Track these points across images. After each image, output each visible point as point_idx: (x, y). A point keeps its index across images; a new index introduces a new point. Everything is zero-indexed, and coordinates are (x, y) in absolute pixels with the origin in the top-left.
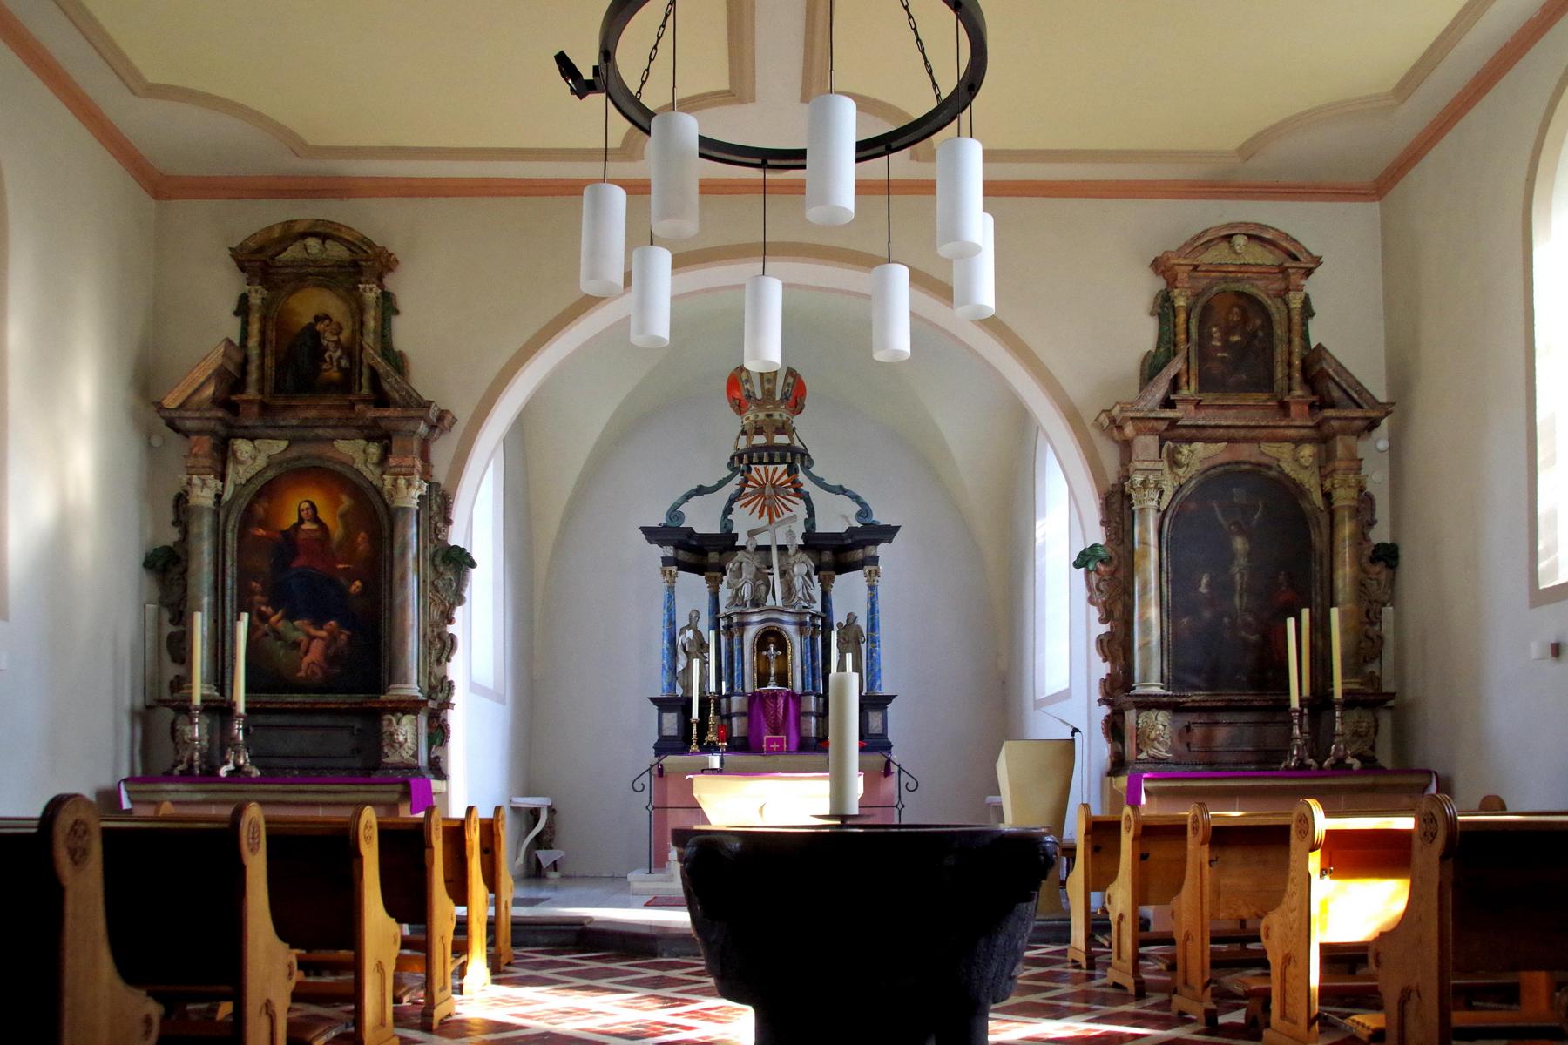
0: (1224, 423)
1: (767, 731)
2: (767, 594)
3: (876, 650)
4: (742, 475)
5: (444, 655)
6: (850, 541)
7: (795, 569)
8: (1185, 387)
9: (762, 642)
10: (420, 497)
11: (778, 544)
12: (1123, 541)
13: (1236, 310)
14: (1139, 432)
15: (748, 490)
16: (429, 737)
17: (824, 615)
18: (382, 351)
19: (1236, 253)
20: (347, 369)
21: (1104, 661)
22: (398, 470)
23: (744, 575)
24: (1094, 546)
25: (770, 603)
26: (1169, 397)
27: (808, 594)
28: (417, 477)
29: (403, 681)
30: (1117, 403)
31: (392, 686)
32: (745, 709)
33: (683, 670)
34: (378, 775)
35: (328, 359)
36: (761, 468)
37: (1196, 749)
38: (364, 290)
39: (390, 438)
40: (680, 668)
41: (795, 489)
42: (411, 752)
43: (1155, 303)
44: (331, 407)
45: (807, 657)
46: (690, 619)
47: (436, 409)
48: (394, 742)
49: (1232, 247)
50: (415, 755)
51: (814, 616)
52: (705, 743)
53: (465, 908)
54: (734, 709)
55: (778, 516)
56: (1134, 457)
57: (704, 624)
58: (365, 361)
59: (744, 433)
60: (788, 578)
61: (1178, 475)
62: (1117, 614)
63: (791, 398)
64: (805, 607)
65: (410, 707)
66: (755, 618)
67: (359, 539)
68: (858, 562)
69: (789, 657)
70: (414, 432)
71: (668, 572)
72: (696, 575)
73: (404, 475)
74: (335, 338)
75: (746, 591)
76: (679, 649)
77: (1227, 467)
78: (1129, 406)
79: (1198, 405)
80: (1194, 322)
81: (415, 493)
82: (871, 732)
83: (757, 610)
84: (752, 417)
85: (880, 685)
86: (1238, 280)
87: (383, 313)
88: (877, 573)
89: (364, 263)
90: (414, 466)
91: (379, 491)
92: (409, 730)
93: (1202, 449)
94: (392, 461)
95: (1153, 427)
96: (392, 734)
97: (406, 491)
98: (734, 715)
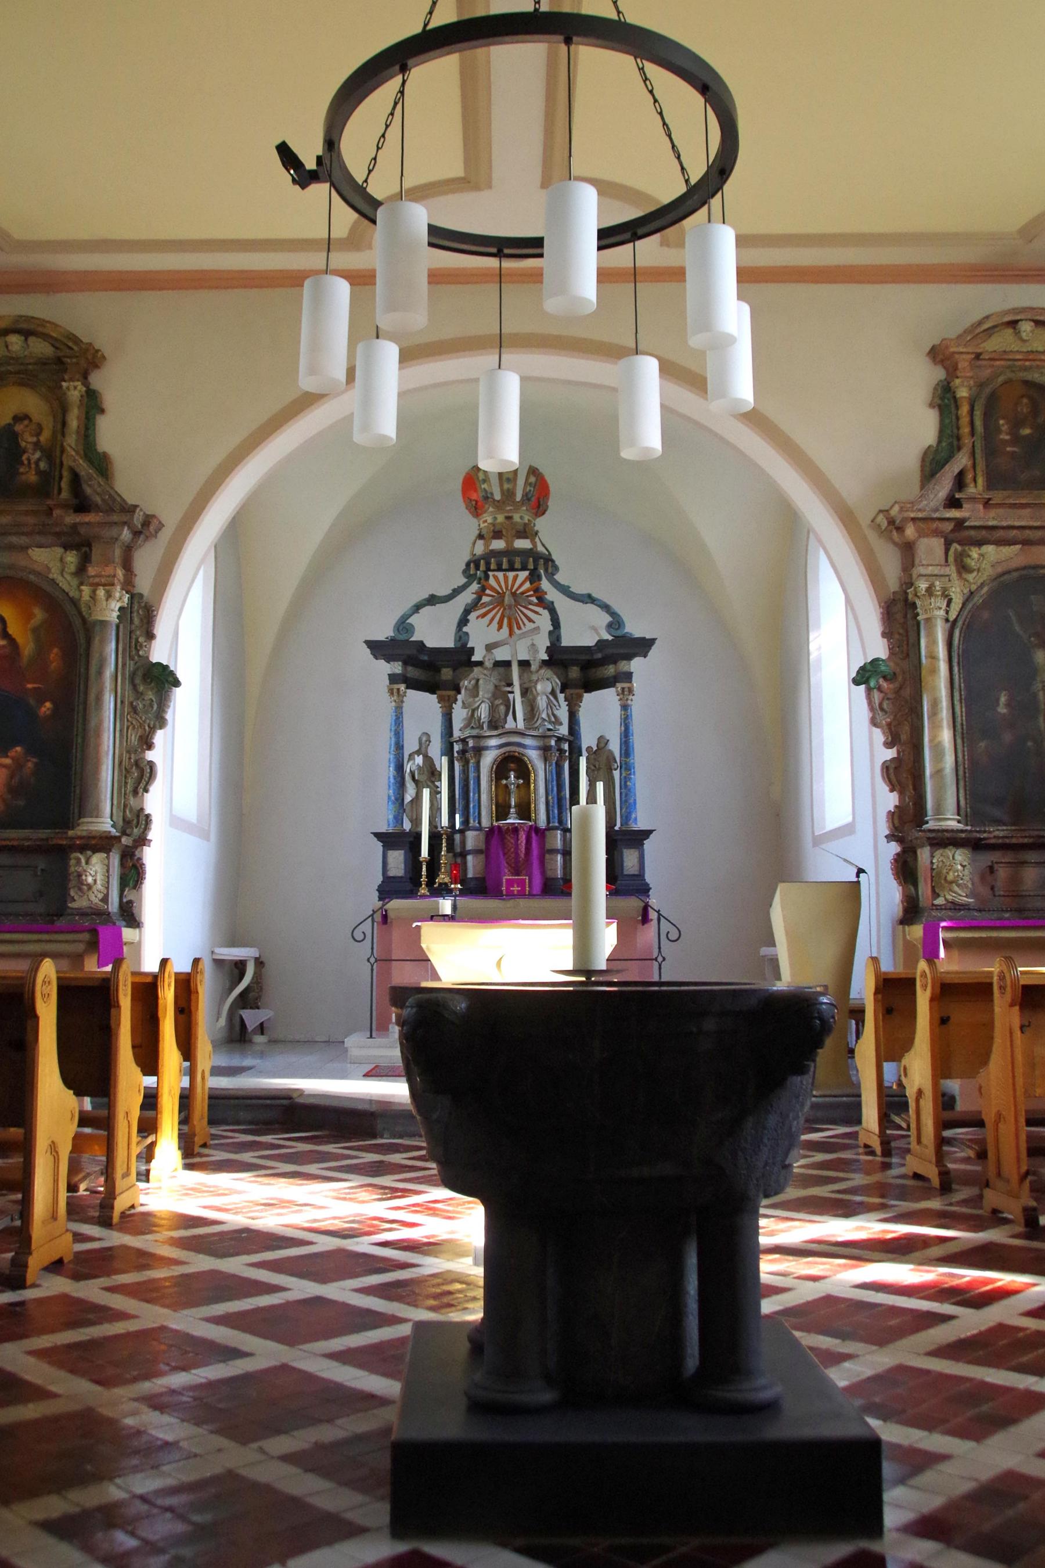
0: (1017, 524)
1: (506, 871)
2: (507, 715)
3: (630, 779)
5: (142, 785)
6: (599, 656)
7: (539, 687)
8: (972, 485)
9: (501, 770)
10: (121, 609)
11: (520, 658)
12: (908, 655)
13: (1025, 400)
14: (922, 534)
15: (485, 599)
16: (121, 878)
17: (571, 738)
18: (84, 451)
19: (1024, 341)
20: (45, 472)
21: (892, 791)
22: (97, 580)
23: (481, 693)
24: (875, 661)
25: (510, 724)
26: (954, 496)
27: (554, 716)
28: (118, 588)
29: (95, 814)
30: (896, 502)
31: (82, 820)
32: (482, 846)
33: (412, 801)
34: (61, 922)
35: (26, 462)
36: (500, 575)
37: (1002, 893)
38: (68, 388)
39: (89, 545)
40: (408, 798)
41: (538, 598)
42: (100, 896)
43: (934, 393)
44: (26, 513)
45: (552, 787)
46: (420, 744)
47: (141, 513)
48: (83, 884)
49: (1017, 333)
50: (105, 899)
51: (560, 739)
52: (436, 886)
53: (155, 1078)
54: (470, 845)
55: (519, 628)
56: (917, 561)
57: (435, 750)
58: (65, 463)
59: (481, 536)
60: (531, 697)
61: (968, 581)
62: (904, 737)
63: (533, 499)
64: (549, 730)
65: (102, 844)
66: (493, 742)
67: (52, 655)
68: (608, 678)
69: (532, 786)
70: (117, 539)
71: (395, 691)
72: (428, 694)
73: (104, 585)
74: (35, 439)
75: (484, 712)
76: (408, 777)
77: (1025, 572)
78: (909, 506)
79: (987, 504)
80: (978, 414)
81: (115, 606)
82: (625, 873)
83: (495, 733)
84: (490, 520)
85: (636, 819)
86: (1026, 369)
87: (87, 413)
88: (631, 691)
89: (69, 360)
90: (114, 576)
91: (75, 603)
92: (99, 870)
93: (993, 552)
94: (91, 571)
95: (937, 529)
96: (79, 875)
97: (104, 603)
98: (469, 852)
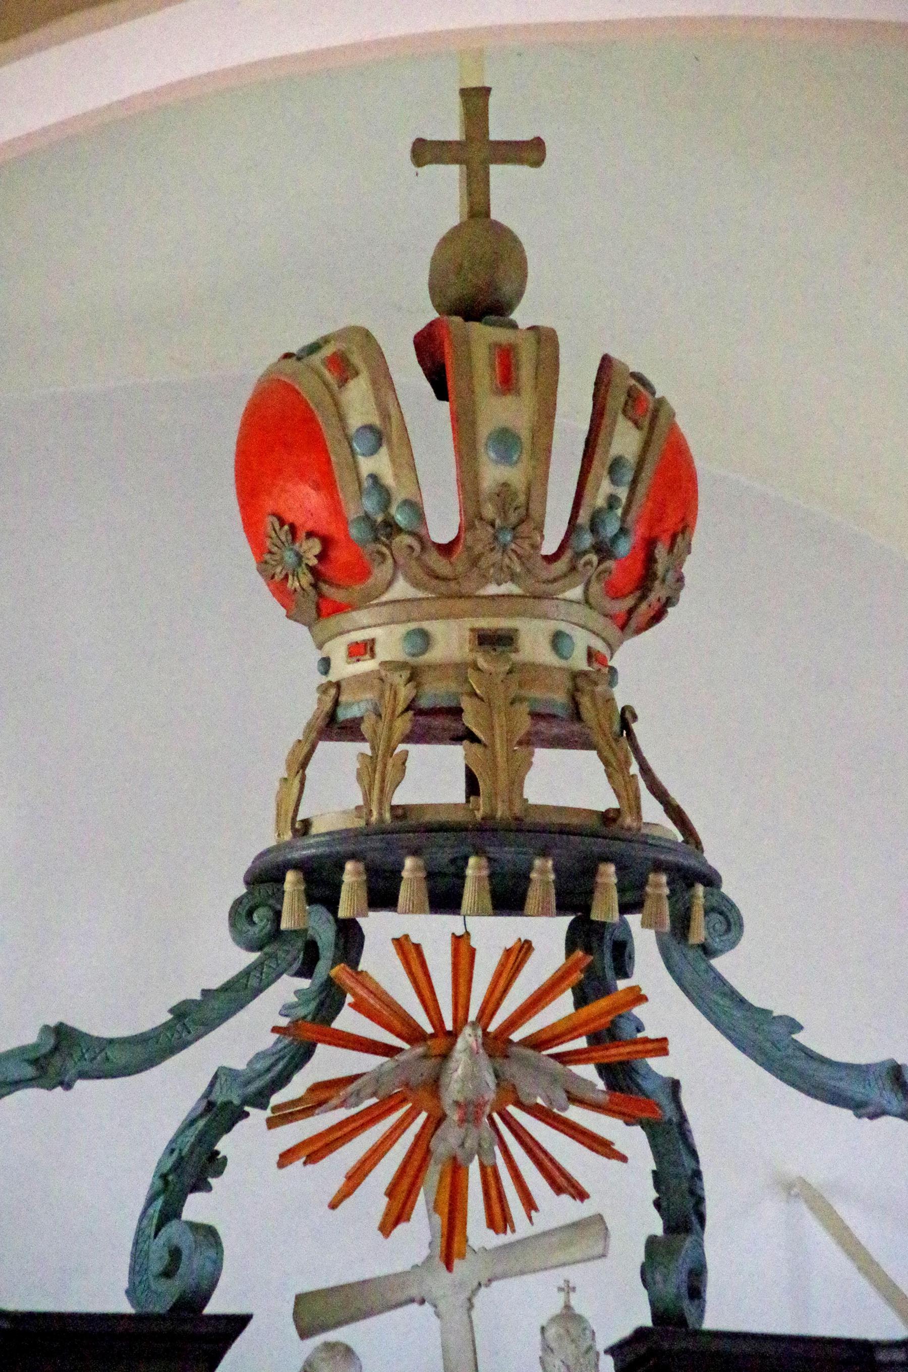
4: (306, 971)
